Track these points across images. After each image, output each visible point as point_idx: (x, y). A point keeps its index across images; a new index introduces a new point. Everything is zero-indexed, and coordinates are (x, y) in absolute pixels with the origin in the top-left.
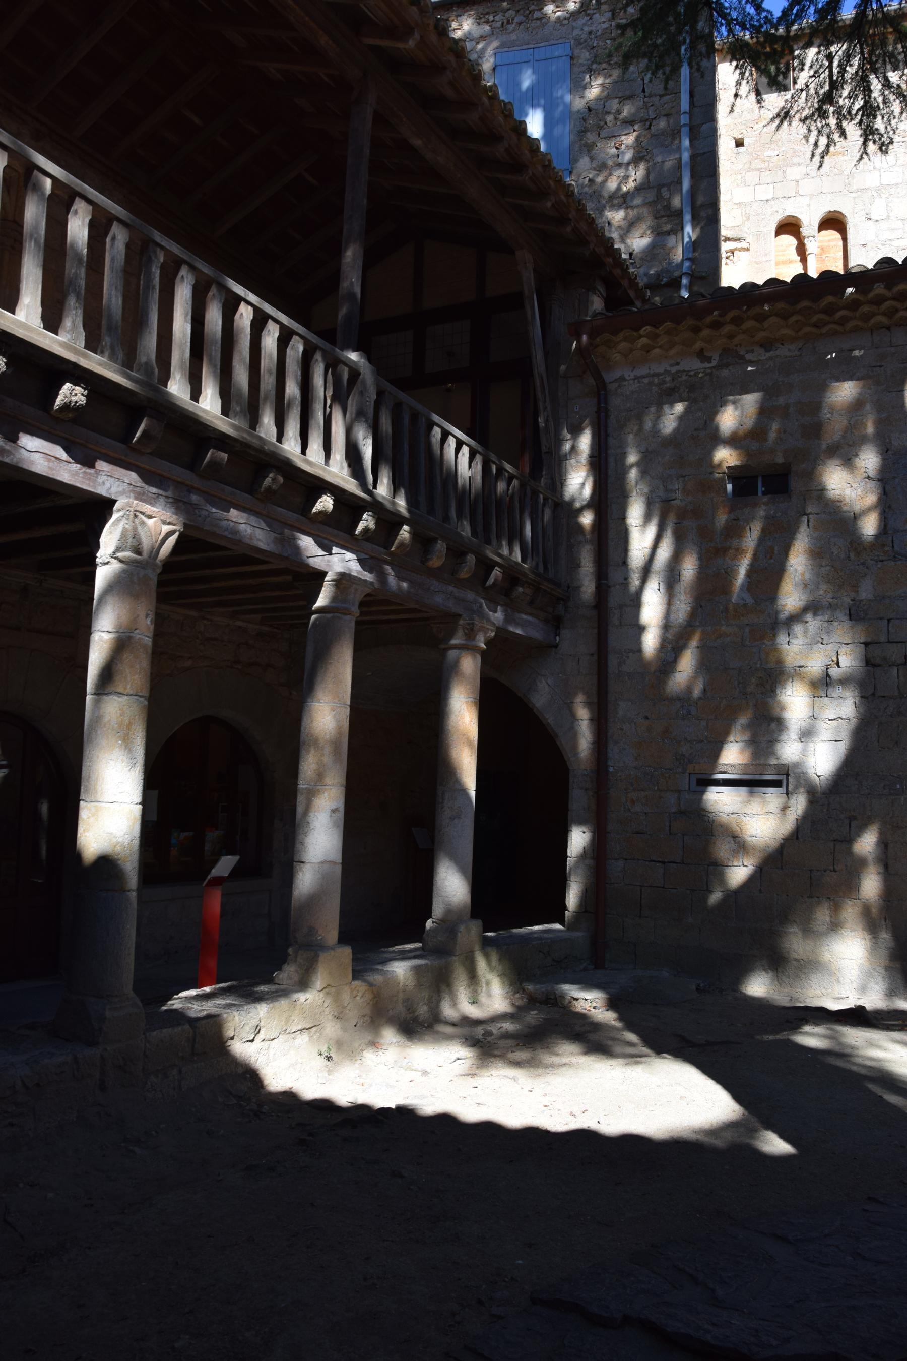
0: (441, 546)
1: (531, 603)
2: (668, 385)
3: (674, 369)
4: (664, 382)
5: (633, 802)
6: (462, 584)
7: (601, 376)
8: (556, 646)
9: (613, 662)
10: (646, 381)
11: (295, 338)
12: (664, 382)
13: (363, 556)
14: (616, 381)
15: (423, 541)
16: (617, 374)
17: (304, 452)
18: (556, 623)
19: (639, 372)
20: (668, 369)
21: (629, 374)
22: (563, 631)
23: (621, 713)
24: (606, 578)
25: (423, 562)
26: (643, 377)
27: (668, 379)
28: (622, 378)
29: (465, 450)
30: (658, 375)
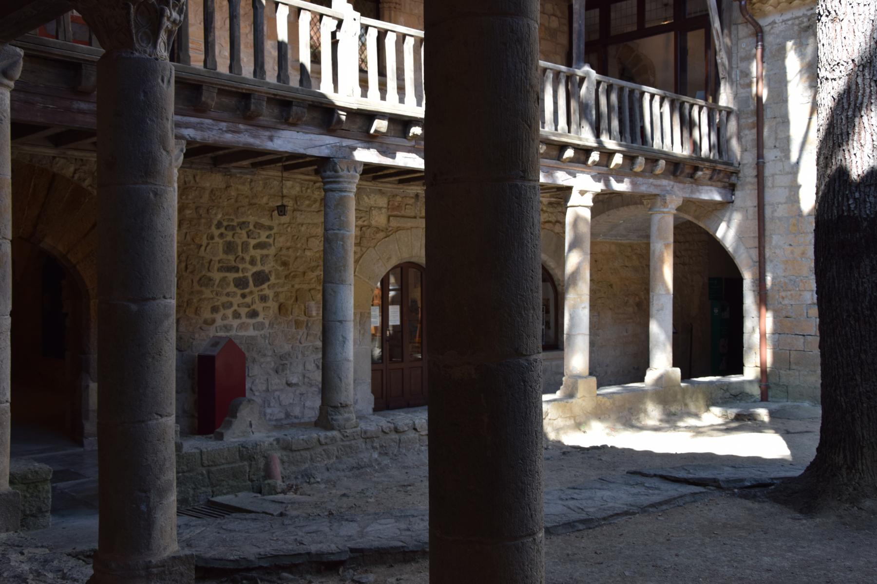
0: (641, 160)
1: (711, 179)
2: (805, 24)
3: (809, 13)
4: (803, 22)
5: (783, 298)
6: (657, 177)
7: (758, 24)
8: (733, 202)
9: (768, 211)
10: (790, 22)
11: (548, 71)
12: (803, 22)
13: (594, 174)
14: (770, 24)
15: (630, 158)
16: (770, 19)
17: (556, 129)
18: (732, 188)
19: (785, 17)
20: (806, 13)
21: (778, 18)
22: (737, 193)
23: (774, 243)
24: (763, 158)
25: (631, 170)
26: (788, 20)
27: (805, 20)
28: (774, 22)
29: (657, 99)
30: (798, 18)
